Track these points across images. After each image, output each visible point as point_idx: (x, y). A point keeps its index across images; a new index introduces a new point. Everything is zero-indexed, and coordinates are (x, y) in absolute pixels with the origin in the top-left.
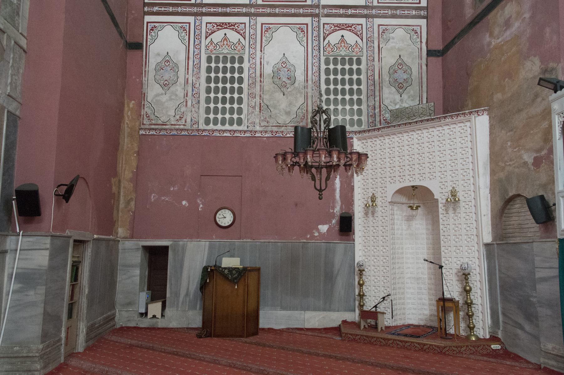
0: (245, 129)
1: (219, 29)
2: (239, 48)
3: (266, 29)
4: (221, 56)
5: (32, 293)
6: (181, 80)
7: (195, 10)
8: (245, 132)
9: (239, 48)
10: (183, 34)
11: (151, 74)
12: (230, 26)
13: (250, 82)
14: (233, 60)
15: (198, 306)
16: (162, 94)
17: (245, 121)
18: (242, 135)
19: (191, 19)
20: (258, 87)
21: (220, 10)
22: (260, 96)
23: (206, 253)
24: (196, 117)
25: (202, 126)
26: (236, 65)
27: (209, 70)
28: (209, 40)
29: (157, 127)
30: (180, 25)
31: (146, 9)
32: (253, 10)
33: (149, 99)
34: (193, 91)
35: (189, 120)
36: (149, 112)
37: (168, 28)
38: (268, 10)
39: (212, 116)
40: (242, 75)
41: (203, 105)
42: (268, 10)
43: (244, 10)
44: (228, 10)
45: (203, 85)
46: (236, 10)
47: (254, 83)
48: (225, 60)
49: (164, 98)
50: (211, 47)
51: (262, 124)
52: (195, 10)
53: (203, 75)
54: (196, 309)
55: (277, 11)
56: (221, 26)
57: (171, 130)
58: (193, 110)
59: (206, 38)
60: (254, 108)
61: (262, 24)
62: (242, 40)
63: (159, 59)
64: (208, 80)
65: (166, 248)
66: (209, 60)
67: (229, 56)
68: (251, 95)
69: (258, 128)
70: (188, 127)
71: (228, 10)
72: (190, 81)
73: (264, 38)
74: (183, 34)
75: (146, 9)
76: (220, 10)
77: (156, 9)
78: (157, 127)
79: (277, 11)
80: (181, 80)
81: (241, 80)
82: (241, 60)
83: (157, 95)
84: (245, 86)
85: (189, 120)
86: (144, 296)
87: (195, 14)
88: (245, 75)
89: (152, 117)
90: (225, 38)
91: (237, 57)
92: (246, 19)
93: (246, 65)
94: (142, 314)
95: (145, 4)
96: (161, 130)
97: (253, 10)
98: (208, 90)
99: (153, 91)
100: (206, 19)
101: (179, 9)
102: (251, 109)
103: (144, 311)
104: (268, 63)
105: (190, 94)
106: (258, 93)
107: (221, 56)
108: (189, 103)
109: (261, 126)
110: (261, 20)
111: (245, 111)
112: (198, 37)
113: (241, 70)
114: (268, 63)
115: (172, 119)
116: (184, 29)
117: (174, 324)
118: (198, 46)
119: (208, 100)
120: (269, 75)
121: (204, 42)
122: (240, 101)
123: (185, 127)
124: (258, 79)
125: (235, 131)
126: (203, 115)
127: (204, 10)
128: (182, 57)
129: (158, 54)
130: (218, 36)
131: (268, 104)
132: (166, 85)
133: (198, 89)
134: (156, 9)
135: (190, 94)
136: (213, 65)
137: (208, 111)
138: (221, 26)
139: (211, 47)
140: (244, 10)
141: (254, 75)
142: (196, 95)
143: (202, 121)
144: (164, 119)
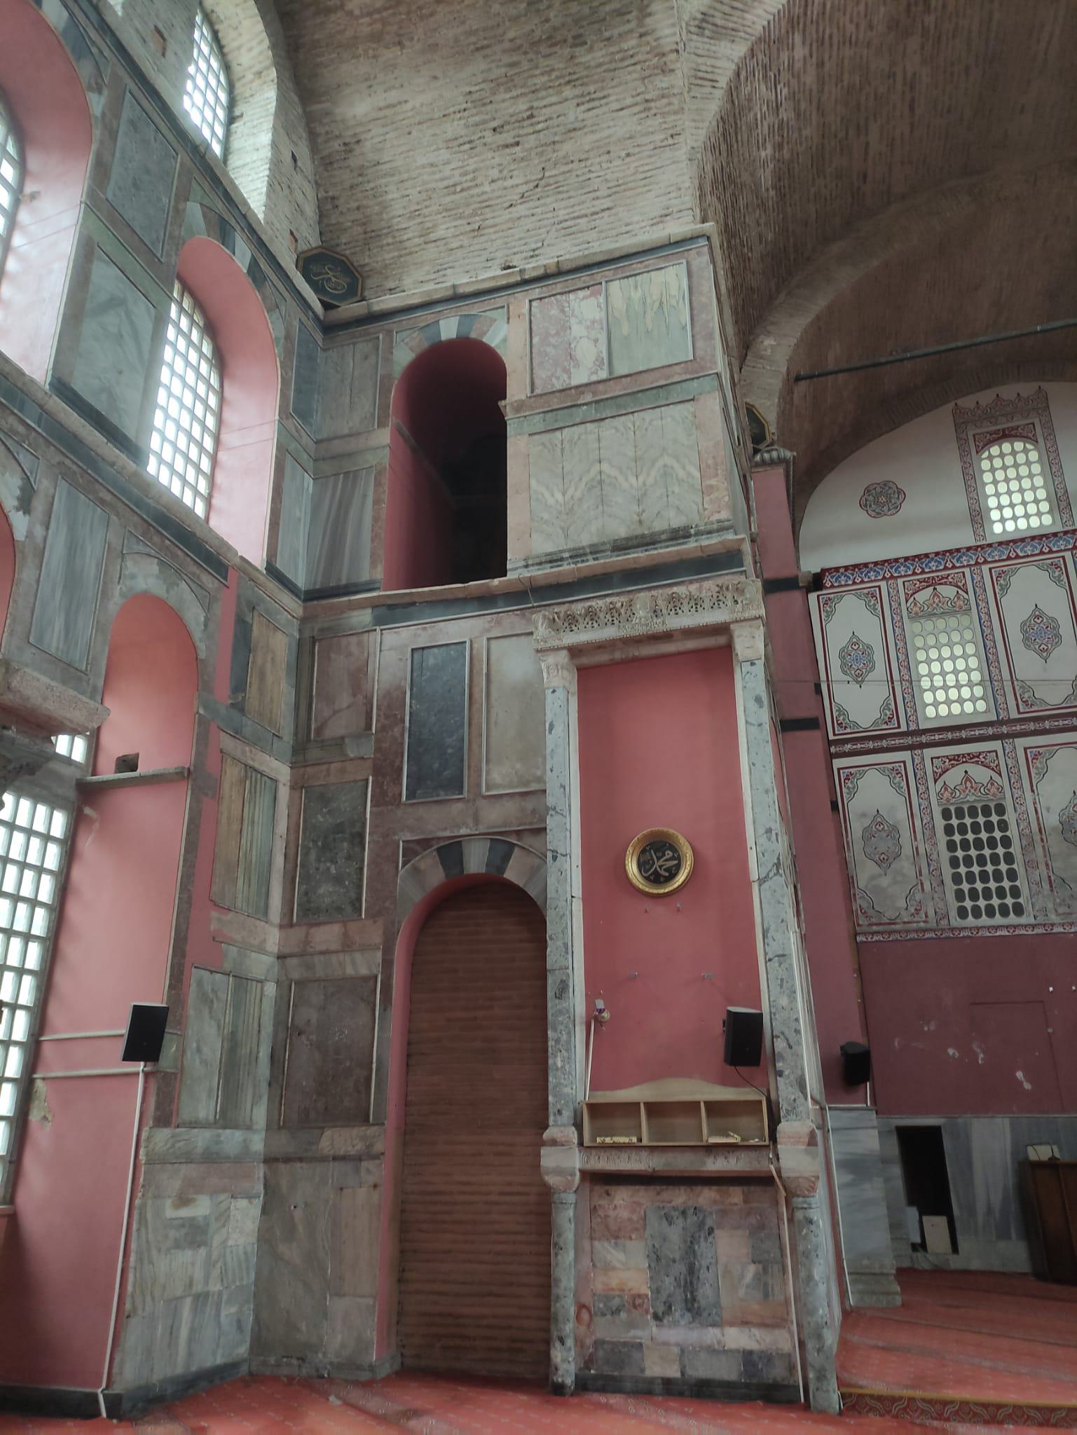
0: (1032, 921)
1: (953, 766)
2: (993, 790)
3: (1033, 756)
4: (966, 807)
5: (867, 1186)
6: (907, 850)
7: (909, 740)
8: (1033, 926)
9: (993, 790)
10: (898, 779)
11: (858, 846)
12: (972, 758)
13: (1024, 842)
14: (986, 811)
15: (1014, 1235)
16: (880, 876)
17: (1028, 907)
18: (1030, 932)
19: (905, 755)
20: (1039, 850)
21: (950, 736)
22: (1047, 865)
23: (1008, 1136)
24: (941, 907)
25: (956, 921)
26: (994, 818)
27: (949, 830)
28: (940, 783)
29: (881, 928)
30: (890, 766)
31: (833, 749)
32: (1005, 729)
33: (862, 884)
34: (929, 865)
35: (931, 913)
36: (864, 905)
37: (872, 774)
38: (1032, 726)
39: (968, 904)
40: (1008, 833)
41: (950, 887)
42: (1032, 726)
43: (990, 731)
44: (964, 734)
45: (945, 855)
46: (977, 733)
47: (1032, 843)
48: (973, 812)
49: (885, 882)
50: (947, 795)
51: (1061, 910)
52: (909, 740)
53: (942, 839)
54: (1010, 1238)
55: (1047, 724)
56: (956, 759)
57: (908, 932)
58: (936, 896)
59: (936, 781)
60: (1039, 884)
61: (1025, 749)
62: (996, 777)
63: (867, 822)
64: (951, 846)
65: (935, 1132)
66: (946, 814)
67: (979, 806)
68: (1030, 864)
69: (1053, 918)
70: (932, 924)
71: (964, 734)
72: (922, 851)
73: (1033, 771)
74: (898, 779)
75: (833, 749)
76: (950, 736)
77: (848, 747)
78: (881, 928)
79: (1047, 724)
80: (907, 850)
81: (1006, 842)
82: (1001, 810)
83: (873, 878)
84: (1015, 849)
85: (931, 913)
86: (913, 1213)
87: (911, 748)
88: (1013, 832)
89: (871, 912)
90: (967, 778)
91: (992, 805)
92: (996, 745)
93: (1010, 816)
94: (914, 1247)
95: (830, 743)
96: (890, 933)
97: (1005, 729)
98: (954, 862)
99: (865, 872)
100: (929, 753)
101: (884, 743)
102: (1034, 887)
103: (917, 1239)
104: (1048, 810)
105: (925, 871)
106: (1041, 860)
107: (966, 807)
108: (927, 887)
109: (1058, 915)
110: (1021, 743)
111: (1025, 891)
112: (921, 780)
113: (1003, 826)
114: (1048, 810)
115: (904, 913)
116: (895, 772)
117: (976, 1265)
118: (924, 795)
119: (957, 879)
120: (1054, 829)
121: (934, 789)
122: (1012, 875)
123: (929, 926)
124: (1037, 837)
125: (1015, 927)
126: (954, 905)
127: (924, 739)
128: (902, 815)
129: (864, 815)
130: (954, 776)
131: (1064, 876)
132: (885, 861)
133: (938, 862)
134: (848, 747)
135: (925, 871)
136: (955, 822)
137: (960, 895)
138: (956, 759)
139: (947, 795)
140: (990, 731)
141: (1027, 831)
142: (936, 873)
143: (953, 913)
144: (890, 914)
